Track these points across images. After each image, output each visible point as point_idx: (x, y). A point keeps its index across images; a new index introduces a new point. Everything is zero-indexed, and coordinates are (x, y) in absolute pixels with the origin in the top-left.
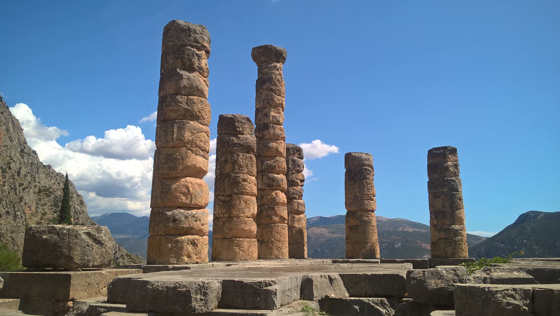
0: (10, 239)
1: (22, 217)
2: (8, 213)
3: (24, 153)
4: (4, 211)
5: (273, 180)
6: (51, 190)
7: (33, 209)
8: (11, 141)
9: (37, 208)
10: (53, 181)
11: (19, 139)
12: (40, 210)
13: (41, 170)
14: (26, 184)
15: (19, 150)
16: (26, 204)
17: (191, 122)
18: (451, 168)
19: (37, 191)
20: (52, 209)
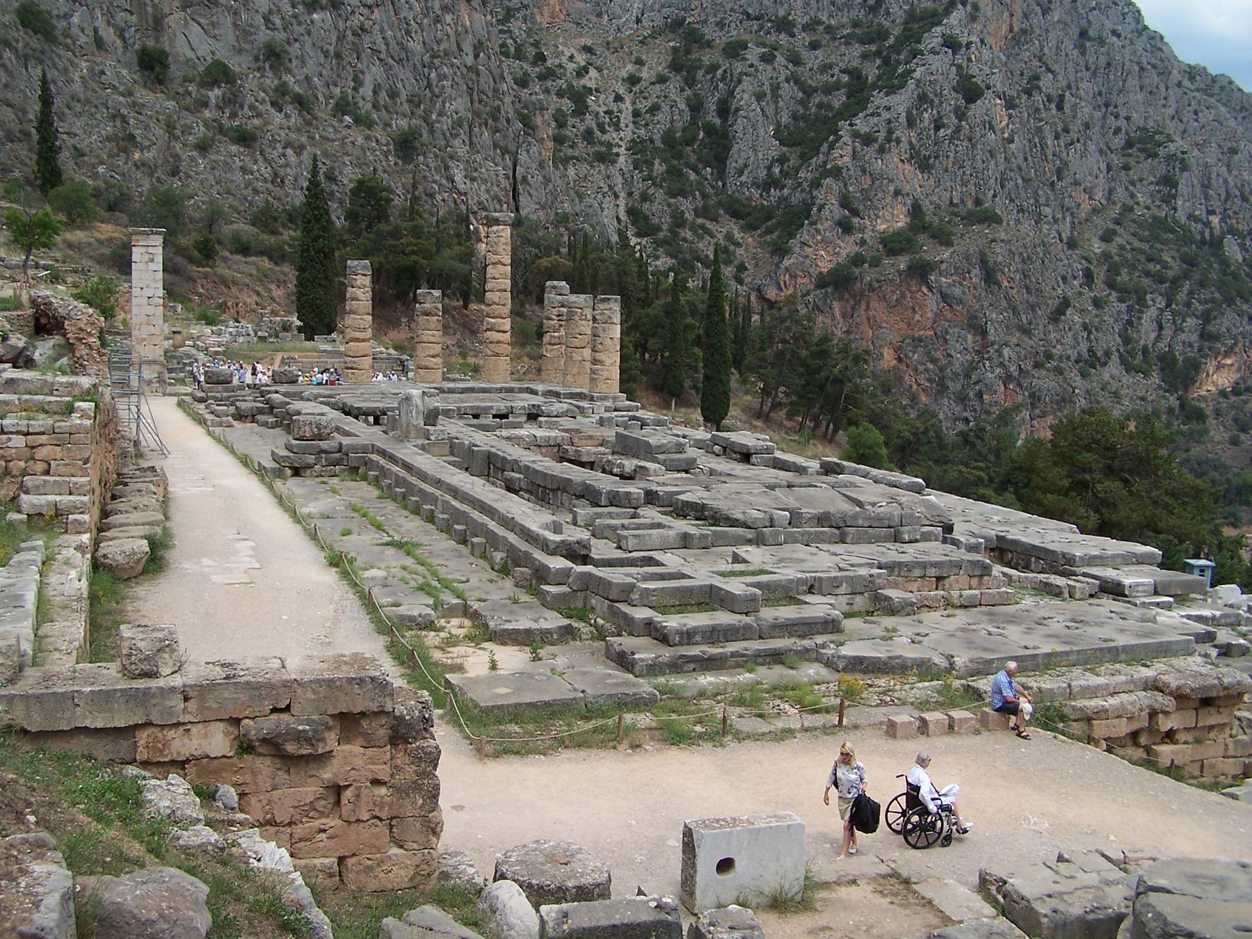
3: (1089, 39)
7: (1099, 195)
10: (1171, 111)
12: (1121, 194)
13: (1132, 83)
15: (1074, 31)
16: (1076, 183)
20: (1159, 192)
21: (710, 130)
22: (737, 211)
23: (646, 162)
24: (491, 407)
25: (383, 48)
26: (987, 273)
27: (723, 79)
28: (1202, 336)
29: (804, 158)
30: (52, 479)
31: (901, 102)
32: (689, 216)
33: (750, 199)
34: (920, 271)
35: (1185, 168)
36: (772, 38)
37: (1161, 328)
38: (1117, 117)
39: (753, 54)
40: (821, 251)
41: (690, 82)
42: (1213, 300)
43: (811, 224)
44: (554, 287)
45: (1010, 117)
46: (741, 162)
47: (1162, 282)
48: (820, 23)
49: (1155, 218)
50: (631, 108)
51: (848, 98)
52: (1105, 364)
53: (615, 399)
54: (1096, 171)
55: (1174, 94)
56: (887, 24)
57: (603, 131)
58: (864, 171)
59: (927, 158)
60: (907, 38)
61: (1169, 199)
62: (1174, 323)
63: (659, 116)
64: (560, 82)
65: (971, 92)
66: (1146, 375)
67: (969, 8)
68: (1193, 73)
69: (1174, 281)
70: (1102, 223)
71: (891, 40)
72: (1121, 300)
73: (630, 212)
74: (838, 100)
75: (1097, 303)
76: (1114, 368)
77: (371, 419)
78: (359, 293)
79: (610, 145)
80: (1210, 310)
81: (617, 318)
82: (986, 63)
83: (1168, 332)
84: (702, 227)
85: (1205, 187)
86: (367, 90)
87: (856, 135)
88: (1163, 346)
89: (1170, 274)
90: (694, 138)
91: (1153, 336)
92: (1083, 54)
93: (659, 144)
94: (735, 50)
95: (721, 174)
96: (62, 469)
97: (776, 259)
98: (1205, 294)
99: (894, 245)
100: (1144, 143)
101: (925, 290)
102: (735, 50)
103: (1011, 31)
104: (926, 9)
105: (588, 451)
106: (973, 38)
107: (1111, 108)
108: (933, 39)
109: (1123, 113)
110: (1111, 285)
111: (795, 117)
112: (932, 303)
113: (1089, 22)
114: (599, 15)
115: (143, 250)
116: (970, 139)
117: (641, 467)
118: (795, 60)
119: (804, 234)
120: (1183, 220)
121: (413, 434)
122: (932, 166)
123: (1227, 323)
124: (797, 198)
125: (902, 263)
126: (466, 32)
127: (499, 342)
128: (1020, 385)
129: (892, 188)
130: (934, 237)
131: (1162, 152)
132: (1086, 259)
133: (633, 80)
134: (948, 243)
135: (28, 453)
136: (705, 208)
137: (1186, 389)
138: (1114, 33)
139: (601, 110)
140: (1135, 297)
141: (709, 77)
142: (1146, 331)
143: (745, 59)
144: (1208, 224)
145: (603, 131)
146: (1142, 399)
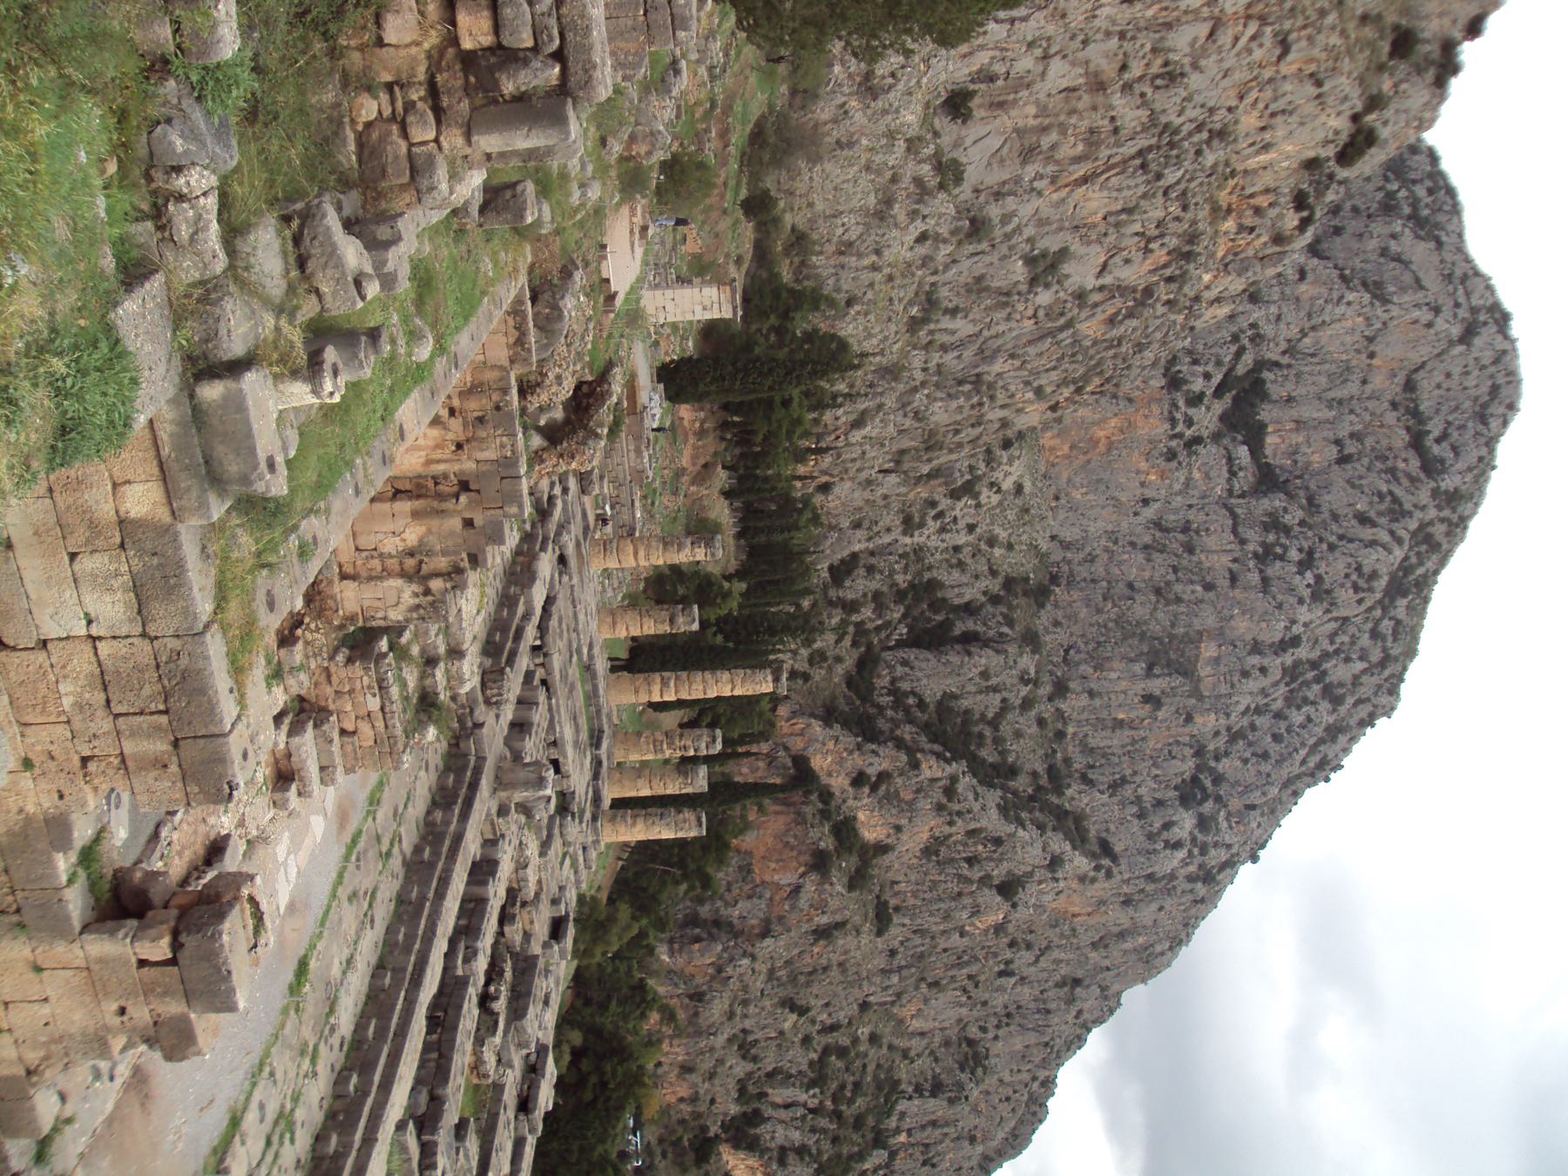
0: (824, 962)
1: (887, 988)
2: (893, 953)
3: (1073, 988)
4: (896, 943)
6: (980, 1071)
7: (916, 1024)
8: (1094, 945)
9: (922, 1034)
10: (1007, 1078)
11: (1108, 969)
13: (1032, 1038)
14: (980, 994)
15: (1079, 974)
16: (926, 1001)
19: (971, 1036)
21: (946, 625)
22: (866, 663)
23: (906, 566)
24: (565, 757)
25: (993, 332)
26: (824, 931)
27: (1001, 635)
28: (783, 1149)
29: (926, 727)
30: (336, 747)
31: (992, 821)
32: (855, 618)
33: (879, 676)
34: (820, 863)
35: (951, 1101)
36: (1046, 678)
37: (787, 1106)
38: (998, 1027)
39: (1027, 662)
40: (832, 755)
41: (995, 600)
42: (820, 1152)
43: (859, 747)
44: (714, 741)
45: (986, 931)
46: (916, 663)
47: (834, 1101)
48: (1065, 723)
49: (898, 1082)
50: (960, 543)
51: (992, 765)
52: (744, 1057)
53: (596, 842)
54: (941, 1018)
55: (1026, 1076)
56: (1069, 792)
57: (935, 518)
58: (918, 791)
59: (937, 853)
60: (1058, 818)
61: (918, 1089)
62: (793, 1119)
63: (956, 574)
64: (982, 465)
65: (1008, 889)
66: (738, 1100)
67: (1092, 874)
68: (1048, 1085)
69: (837, 1115)
70: (886, 1030)
71: (1054, 799)
72: (811, 1064)
73: (854, 556)
74: (988, 754)
75: (806, 1040)
76: (741, 1068)
77: (538, 643)
78: (687, 551)
79: (922, 525)
80: (810, 1155)
81: (680, 835)
82: (1039, 897)
83: (783, 1114)
84: (845, 633)
85: (934, 1124)
86: (946, 323)
87: (954, 779)
88: (768, 1112)
89: (843, 1108)
90: (935, 613)
91: (778, 1100)
92: (1057, 985)
93: (927, 575)
94: (1031, 640)
95: (900, 644)
96: (349, 748)
97: (820, 711)
98: (826, 1146)
99: (845, 830)
100: (973, 1057)
101: (802, 870)
102: (1031, 640)
103: (1074, 915)
104: (1087, 831)
105: (514, 933)
106: (1062, 884)
107: (1005, 1020)
108: (1059, 844)
109: (1001, 1033)
110: (826, 1051)
111: (967, 712)
112: (787, 878)
113: (1088, 987)
114: (1057, 498)
115: (715, 298)
116: (960, 894)
117: (496, 1023)
118: (1027, 704)
119: (849, 740)
120: (900, 1107)
121: (503, 794)
122: (929, 860)
123: (798, 1170)
124: (882, 724)
125: (828, 843)
126: (1019, 411)
127: (650, 692)
128: (713, 978)
129: (904, 822)
130: (857, 871)
131: (964, 1077)
132: (850, 1023)
133: (992, 542)
134: (851, 887)
135: (363, 712)
136: (867, 632)
137: (727, 1141)
138: (1080, 1012)
139: (957, 512)
140: (817, 1077)
141: (1000, 619)
142: (779, 1094)
143: (1021, 655)
144: (897, 1131)
145: (935, 518)
146: (713, 1101)
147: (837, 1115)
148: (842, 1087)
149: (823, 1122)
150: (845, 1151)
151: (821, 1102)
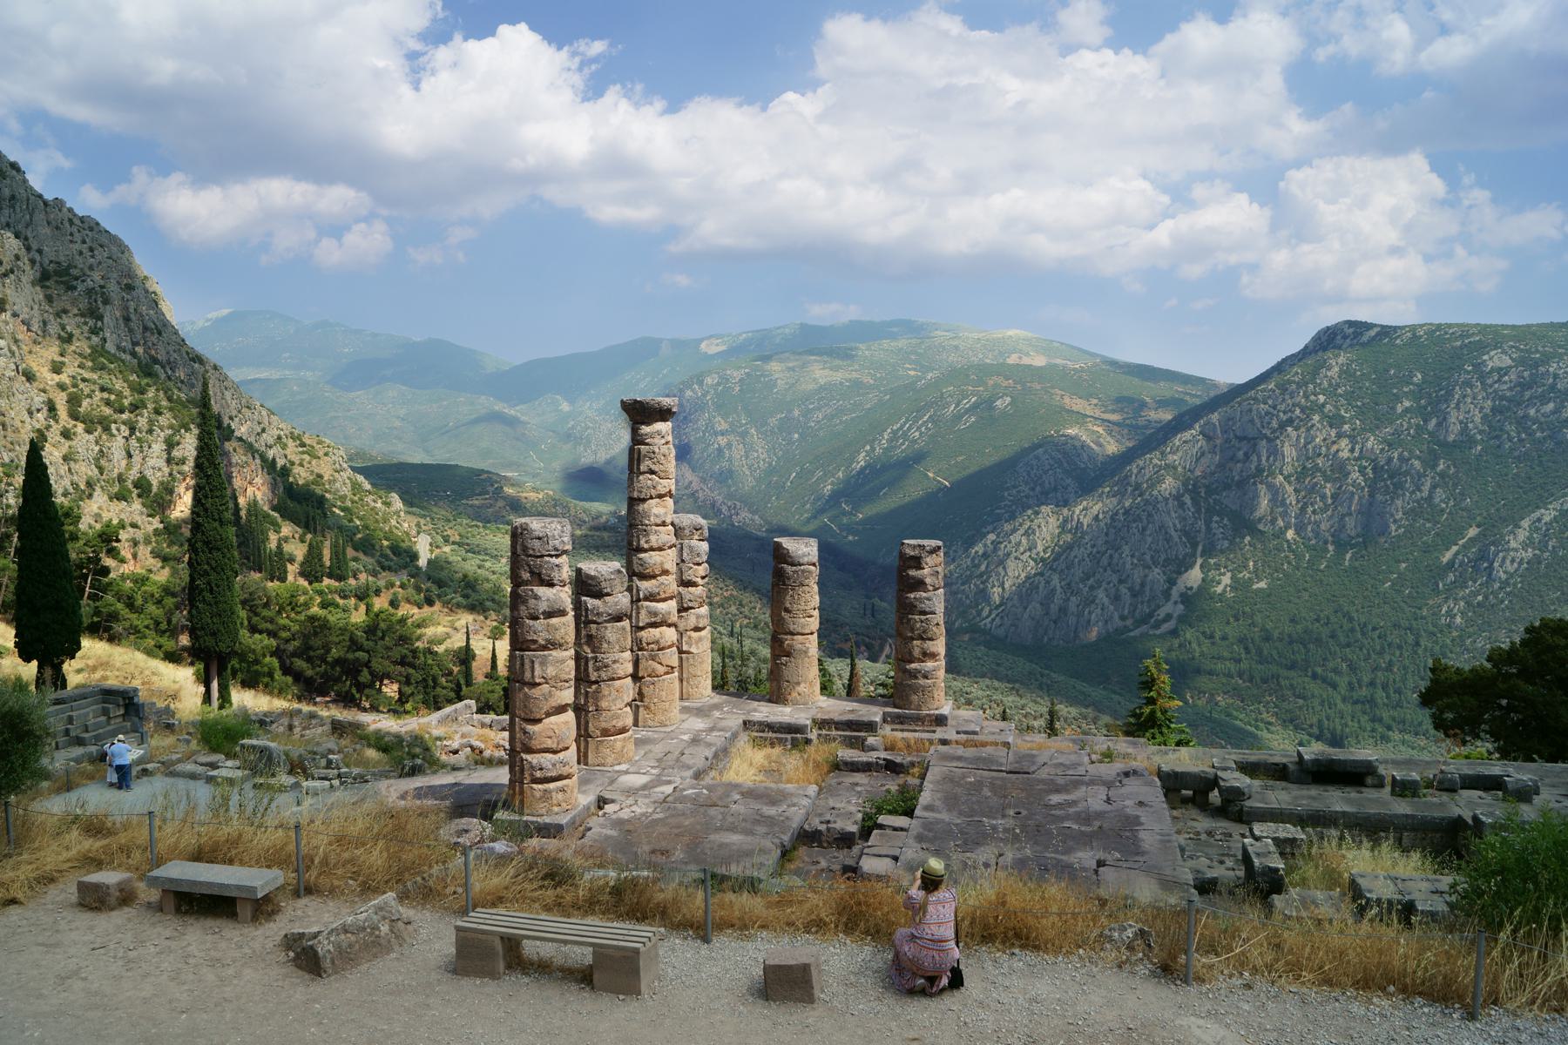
5: (656, 614)
17: (554, 653)
18: (928, 580)
28: (169, 461)
37: (130, 456)
42: (171, 427)
47: (122, 411)
52: (90, 496)
69: (134, 408)
72: (89, 431)
75: (66, 434)
83: (137, 458)
88: (133, 474)
89: (126, 402)
91: (124, 463)
110: (74, 416)
132: (44, 391)
142: (118, 462)
144: (134, 354)
147: (134, 408)
148: (108, 403)
149: (142, 422)
150: (164, 403)
151: (124, 423)
